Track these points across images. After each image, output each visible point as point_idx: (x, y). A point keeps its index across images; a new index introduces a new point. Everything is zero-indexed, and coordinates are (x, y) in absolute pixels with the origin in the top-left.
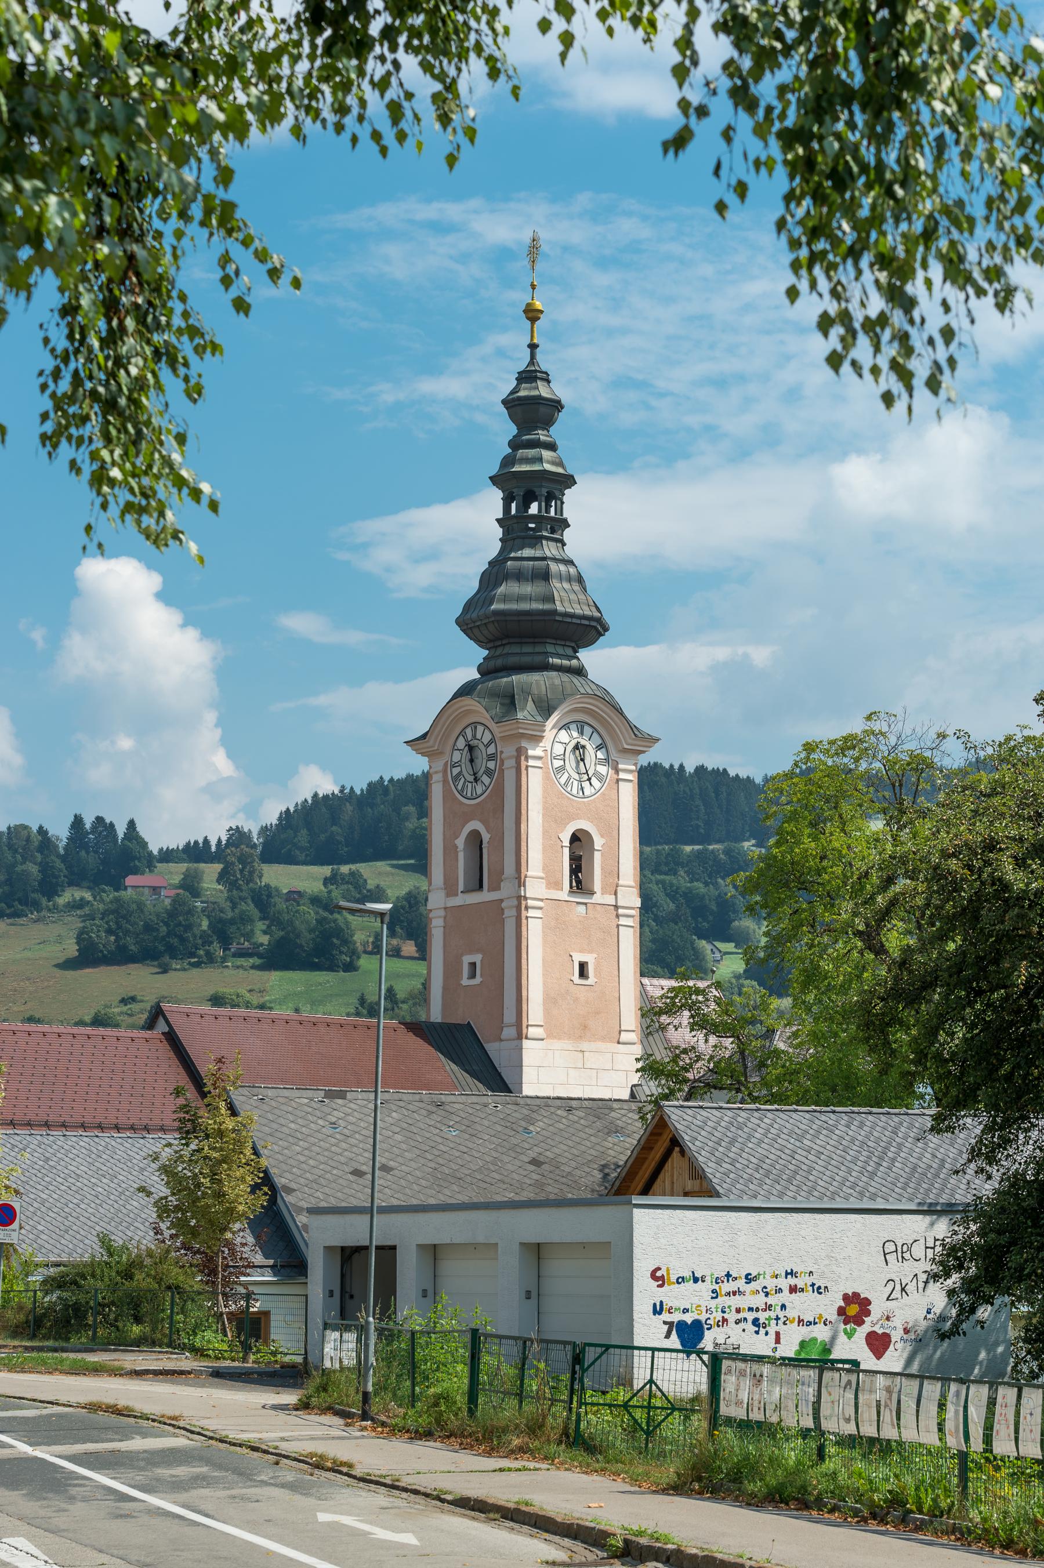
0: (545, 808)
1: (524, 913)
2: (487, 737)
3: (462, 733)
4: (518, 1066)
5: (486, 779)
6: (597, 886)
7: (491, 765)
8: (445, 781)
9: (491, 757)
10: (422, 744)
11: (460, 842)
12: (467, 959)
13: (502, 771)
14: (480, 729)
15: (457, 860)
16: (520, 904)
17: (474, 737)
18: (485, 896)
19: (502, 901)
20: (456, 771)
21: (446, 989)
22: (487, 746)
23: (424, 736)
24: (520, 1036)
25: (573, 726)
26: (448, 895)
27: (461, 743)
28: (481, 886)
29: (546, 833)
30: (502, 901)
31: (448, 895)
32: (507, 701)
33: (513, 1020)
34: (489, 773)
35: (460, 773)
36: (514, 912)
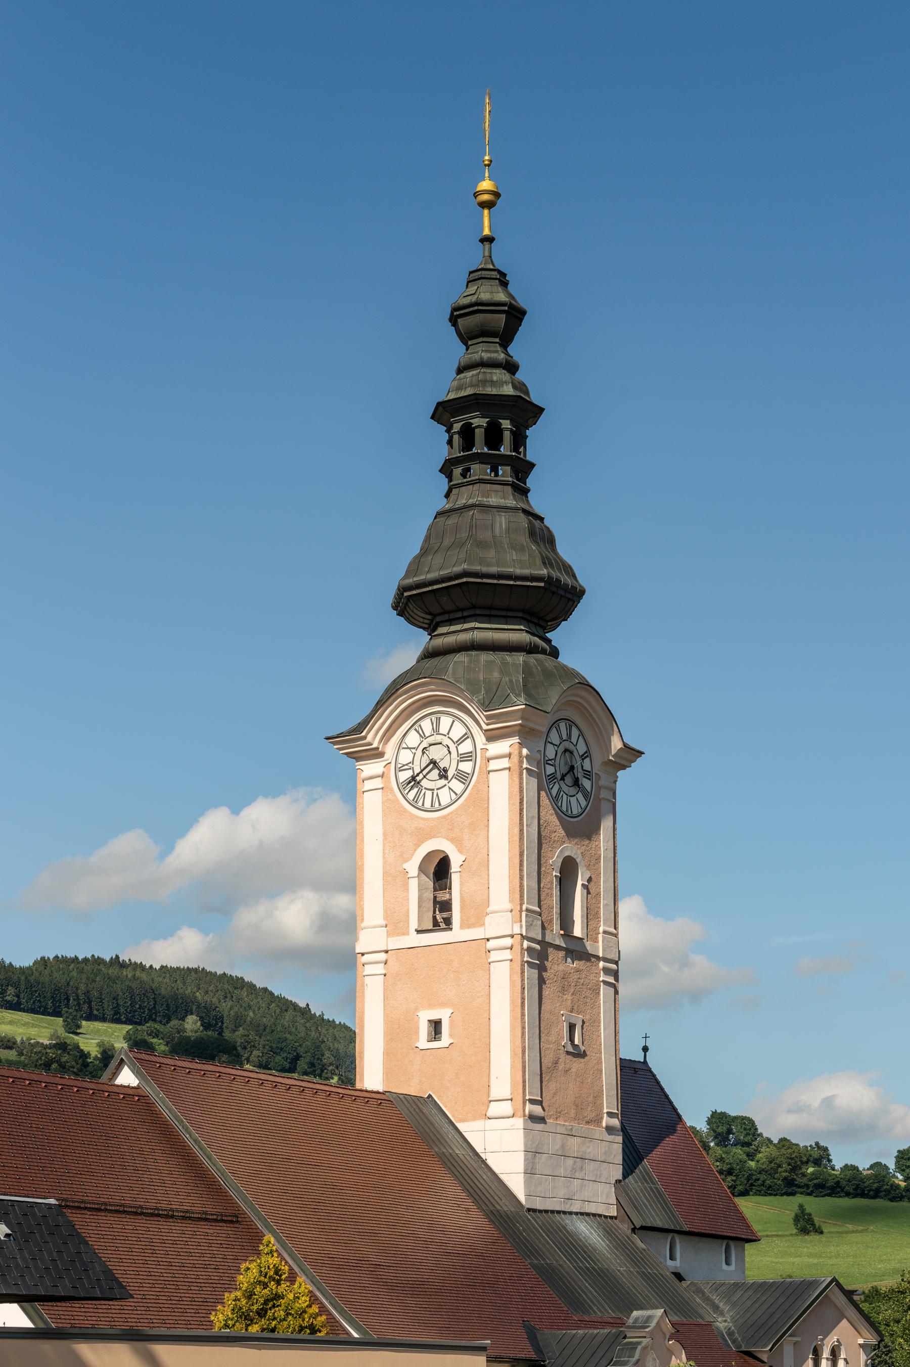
7: (466, 767)
9: (464, 758)
11: (412, 867)
12: (425, 1016)
17: (436, 730)
18: (457, 933)
21: (388, 1054)
25: (562, 725)
28: (448, 922)
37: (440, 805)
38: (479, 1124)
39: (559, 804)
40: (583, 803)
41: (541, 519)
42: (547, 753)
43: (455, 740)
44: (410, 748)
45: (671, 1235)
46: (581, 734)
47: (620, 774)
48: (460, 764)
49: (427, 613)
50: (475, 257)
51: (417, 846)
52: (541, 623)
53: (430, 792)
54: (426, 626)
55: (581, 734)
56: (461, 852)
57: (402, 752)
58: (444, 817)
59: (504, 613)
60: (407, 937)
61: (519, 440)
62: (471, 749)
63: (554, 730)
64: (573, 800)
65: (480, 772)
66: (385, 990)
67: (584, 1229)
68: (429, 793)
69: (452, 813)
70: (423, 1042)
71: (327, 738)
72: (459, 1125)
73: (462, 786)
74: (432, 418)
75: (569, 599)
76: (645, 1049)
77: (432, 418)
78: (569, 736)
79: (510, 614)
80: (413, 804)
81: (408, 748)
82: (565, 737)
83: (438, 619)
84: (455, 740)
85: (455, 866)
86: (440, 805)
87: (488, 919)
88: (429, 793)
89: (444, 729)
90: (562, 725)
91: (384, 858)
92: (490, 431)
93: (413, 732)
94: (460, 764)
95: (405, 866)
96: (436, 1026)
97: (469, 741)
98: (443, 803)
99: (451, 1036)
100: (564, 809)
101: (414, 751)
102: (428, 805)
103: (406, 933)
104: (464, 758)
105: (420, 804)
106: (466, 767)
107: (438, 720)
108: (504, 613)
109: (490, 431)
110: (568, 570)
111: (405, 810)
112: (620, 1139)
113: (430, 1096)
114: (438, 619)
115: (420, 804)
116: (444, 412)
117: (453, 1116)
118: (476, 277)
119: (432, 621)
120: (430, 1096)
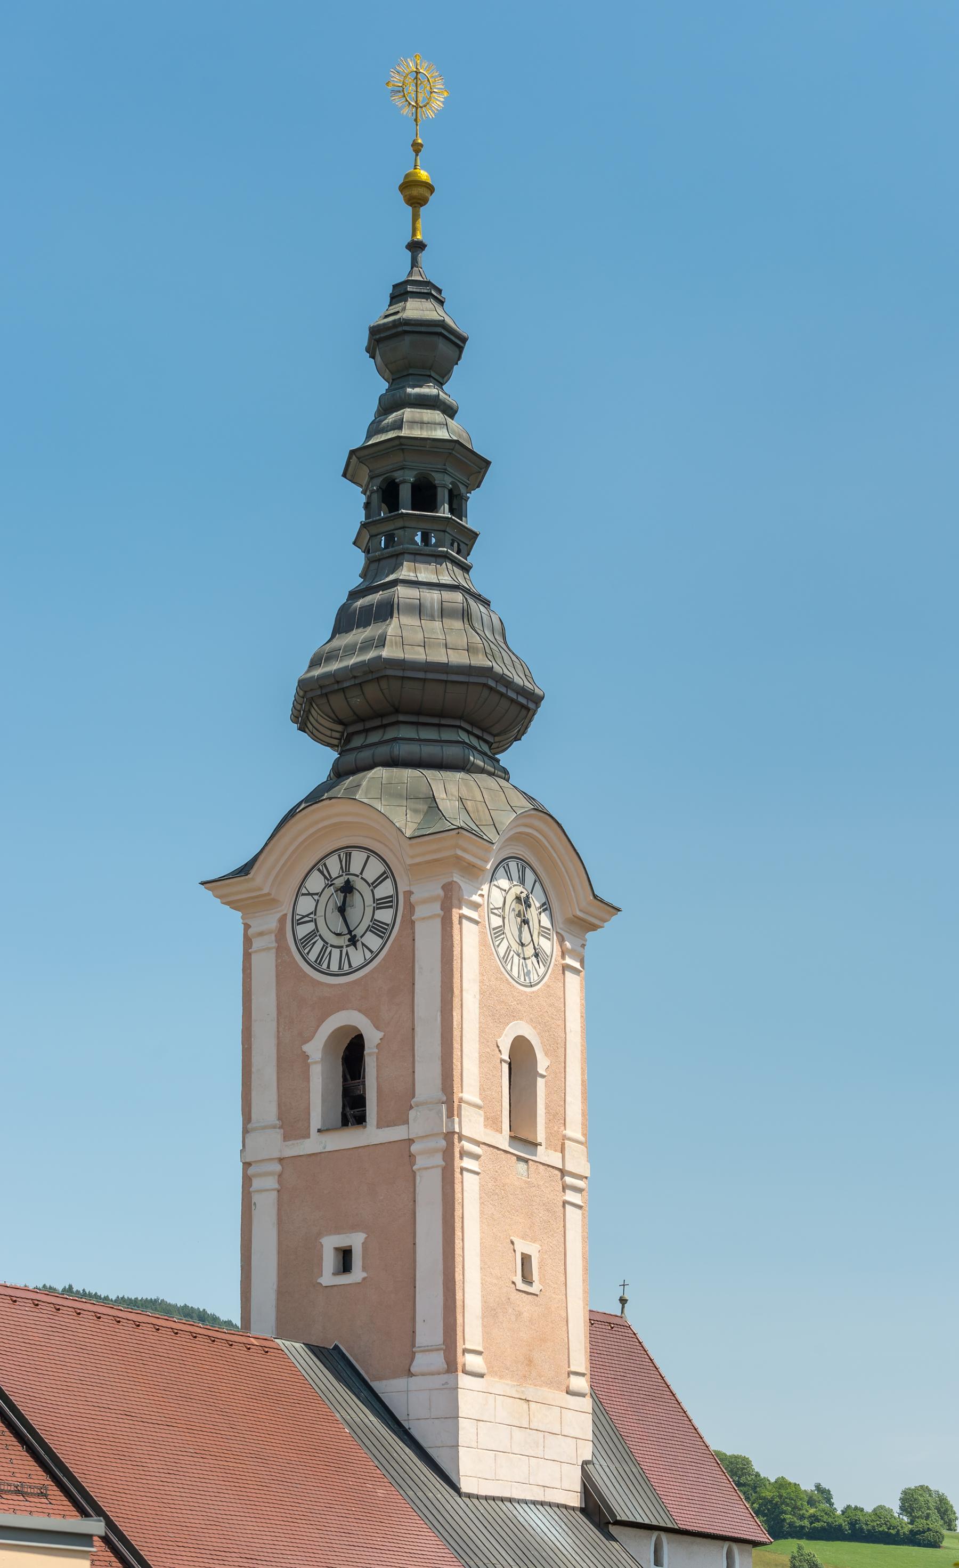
0: (482, 993)
1: (458, 1163)
2: (374, 869)
3: (320, 866)
4: (454, 1417)
5: (373, 941)
6: (541, 1137)
7: (385, 916)
8: (281, 948)
9: (381, 904)
10: (240, 886)
11: (315, 1049)
12: (330, 1244)
13: (410, 924)
14: (358, 858)
15: (307, 1078)
16: (450, 1145)
17: (346, 869)
18: (372, 1134)
19: (411, 1141)
20: (303, 931)
21: (283, 1293)
22: (374, 885)
23: (245, 870)
24: (451, 1367)
25: (513, 865)
26: (286, 1138)
27: (316, 883)
28: (361, 1120)
29: (482, 1031)
30: (411, 1141)
31: (286, 1138)
32: (423, 807)
33: (438, 1339)
34: (378, 929)
35: (314, 933)
36: (438, 1160)
37: (350, 966)
38: (398, 1384)
41: (487, 603)
42: (491, 900)
43: (370, 882)
44: (312, 895)
45: (655, 1534)
46: (538, 879)
47: (590, 935)
48: (377, 912)
49: (335, 722)
51: (321, 1020)
52: (487, 737)
53: (338, 950)
54: (336, 742)
56: (377, 1028)
57: (302, 899)
58: (355, 982)
59: (435, 721)
60: (307, 1141)
61: (457, 504)
63: (501, 871)
65: (402, 922)
66: (279, 1210)
67: (538, 1521)
68: (336, 953)
69: (366, 976)
70: (328, 1277)
71: (203, 883)
72: (375, 1385)
73: (379, 941)
74: (344, 475)
75: (522, 706)
76: (416, 247)
77: (344, 475)
79: (443, 722)
80: (316, 966)
81: (309, 894)
83: (351, 729)
84: (370, 882)
86: (350, 966)
87: (412, 1114)
88: (336, 953)
89: (355, 868)
90: (513, 865)
91: (278, 1038)
93: (316, 873)
94: (377, 912)
95: (305, 1048)
96: (345, 1258)
97: (388, 882)
98: (355, 964)
99: (364, 1269)
100: (515, 974)
101: (316, 897)
102: (334, 967)
103: (307, 1136)
104: (381, 904)
105: (325, 966)
106: (385, 916)
107: (349, 855)
108: (435, 721)
111: (306, 975)
112: (587, 1404)
113: (336, 1347)
114: (351, 729)
115: (325, 966)
117: (367, 1373)
118: (400, 294)
119: (343, 733)
120: (336, 1347)
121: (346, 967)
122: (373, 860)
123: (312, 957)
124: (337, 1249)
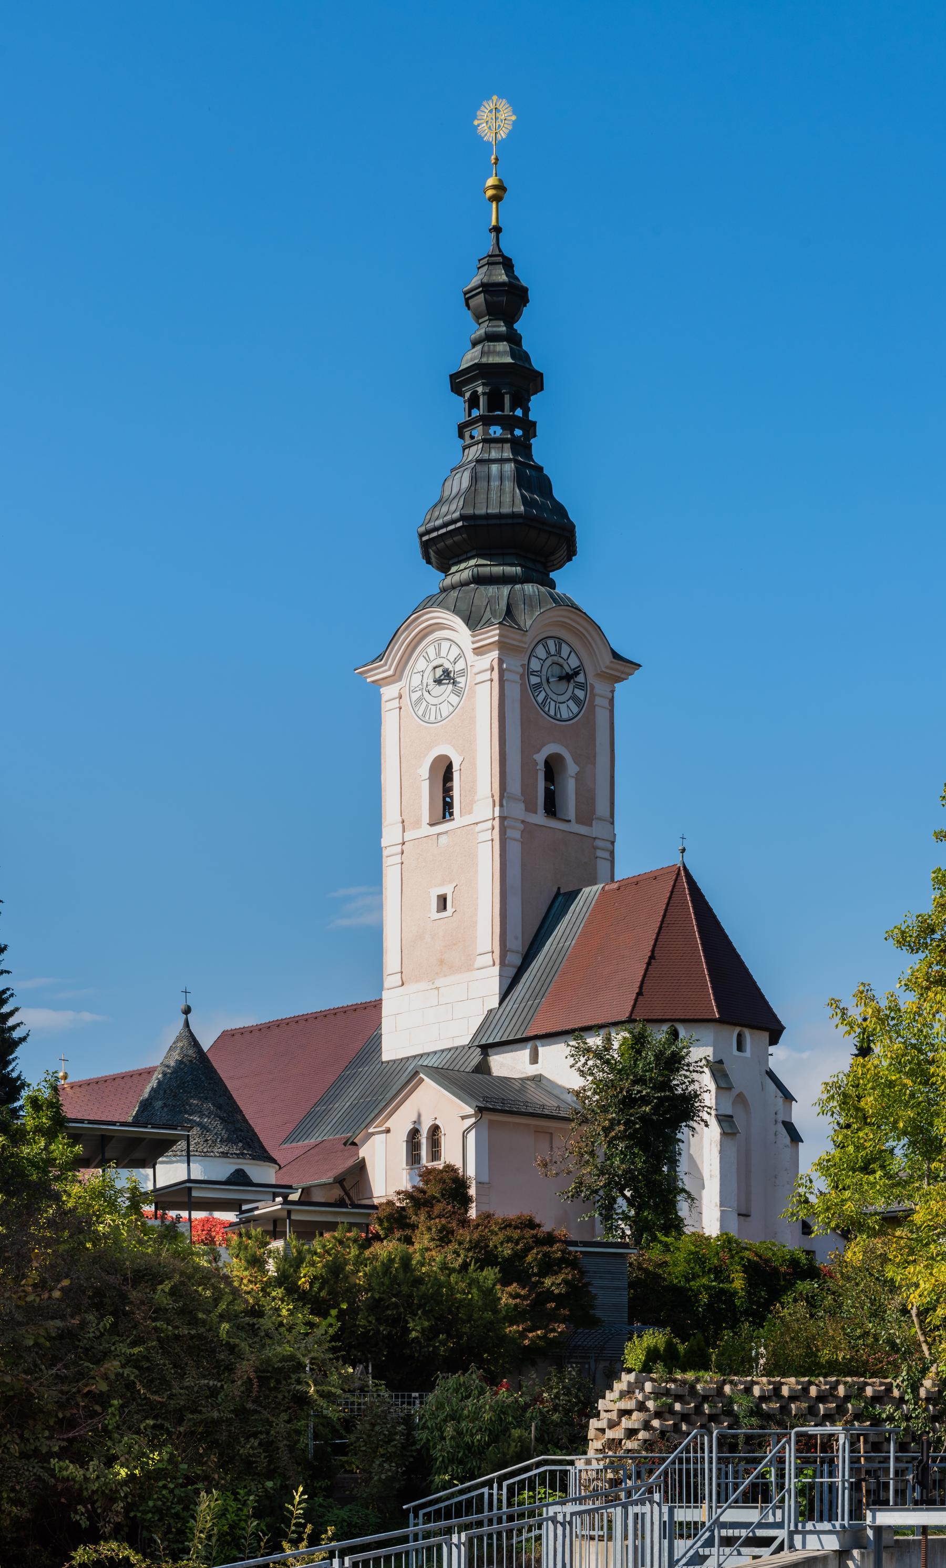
11: (425, 772)
14: (445, 645)
17: (438, 655)
25: (551, 643)
39: (547, 709)
40: (575, 709)
46: (572, 650)
50: (487, 245)
55: (572, 650)
57: (414, 675)
62: (464, 666)
64: (563, 707)
70: (435, 915)
73: (458, 699)
78: (559, 652)
82: (553, 651)
85: (456, 767)
89: (443, 654)
90: (551, 643)
92: (503, 392)
96: (443, 902)
100: (552, 713)
102: (432, 719)
107: (439, 645)
109: (503, 392)
110: (561, 510)
116: (458, 382)
121: (439, 718)
122: (454, 646)
123: (420, 713)
124: (439, 896)
